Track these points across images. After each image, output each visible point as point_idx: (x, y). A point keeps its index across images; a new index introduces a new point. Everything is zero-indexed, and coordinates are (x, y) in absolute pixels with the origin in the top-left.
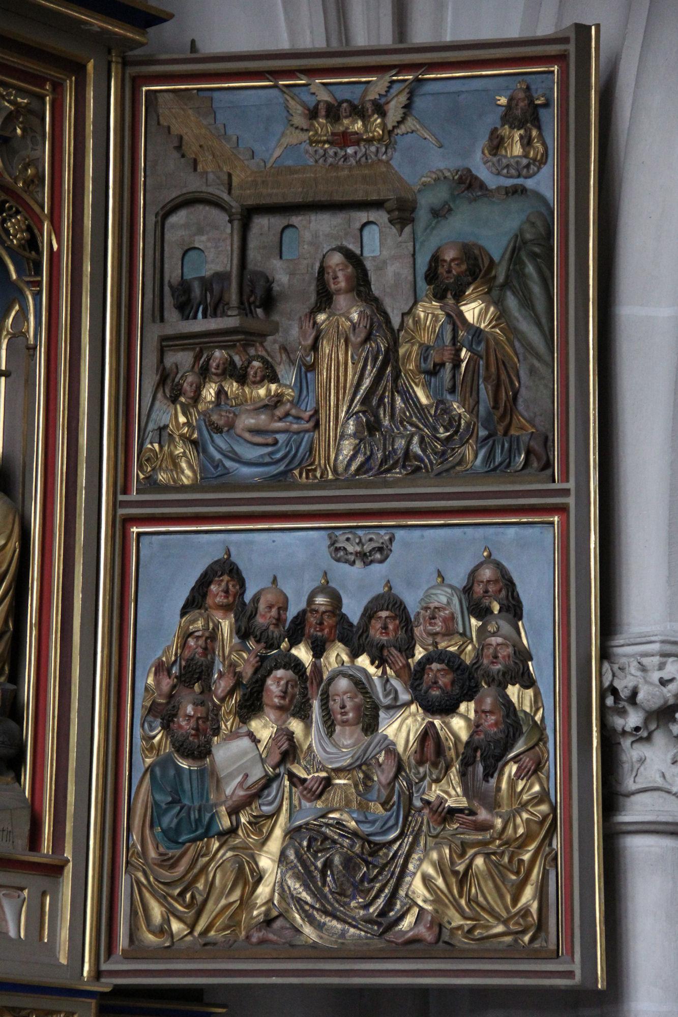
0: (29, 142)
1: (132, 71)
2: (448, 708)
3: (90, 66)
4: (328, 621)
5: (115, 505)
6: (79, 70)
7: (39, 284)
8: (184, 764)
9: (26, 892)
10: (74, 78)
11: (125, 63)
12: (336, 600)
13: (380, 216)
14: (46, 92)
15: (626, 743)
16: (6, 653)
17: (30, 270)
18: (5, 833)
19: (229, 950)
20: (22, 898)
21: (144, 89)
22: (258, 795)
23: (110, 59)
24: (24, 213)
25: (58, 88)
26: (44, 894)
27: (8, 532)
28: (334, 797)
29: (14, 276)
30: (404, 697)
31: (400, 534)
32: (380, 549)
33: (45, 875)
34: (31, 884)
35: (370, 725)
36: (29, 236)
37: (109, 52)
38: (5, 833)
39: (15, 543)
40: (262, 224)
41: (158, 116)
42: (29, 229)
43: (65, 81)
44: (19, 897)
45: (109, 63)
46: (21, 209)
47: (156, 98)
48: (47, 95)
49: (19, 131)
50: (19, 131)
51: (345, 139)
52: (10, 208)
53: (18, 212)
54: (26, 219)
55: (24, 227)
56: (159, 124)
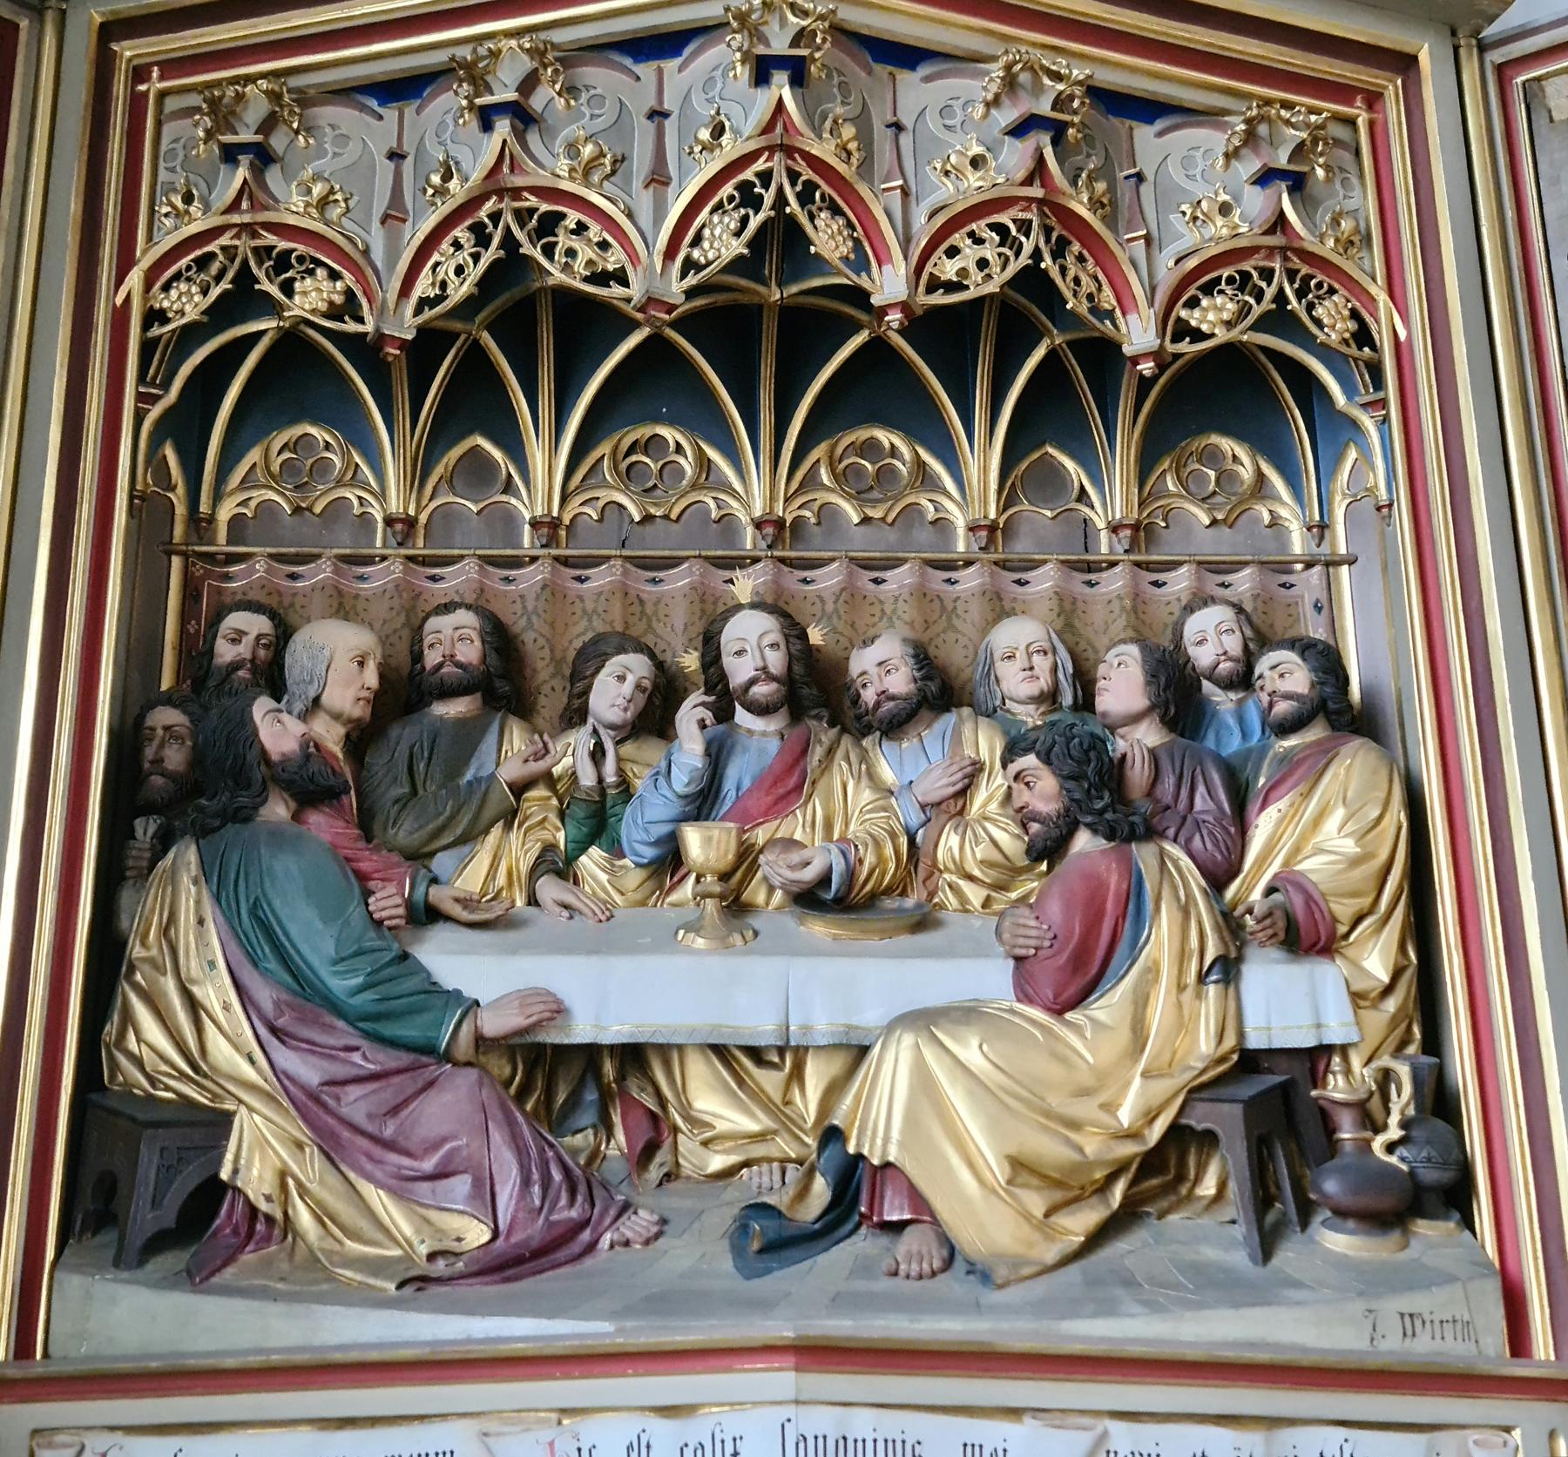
0: (1338, 186)
1: (1497, 56)
3: (1424, 58)
6: (1405, 64)
7: (1383, 403)
9: (1517, 1434)
10: (1399, 82)
11: (1483, 48)
14: (1356, 111)
16: (1411, 1005)
17: (1365, 386)
18: (1459, 1326)
20: (1511, 1444)
21: (1520, 80)
23: (1456, 42)
24: (1342, 291)
25: (1373, 99)
26: (1552, 1435)
27: (1383, 795)
29: (1340, 398)
33: (1547, 1400)
36: (1356, 326)
37: (1454, 33)
38: (1459, 1326)
39: (1398, 815)
41: (1550, 111)
42: (1355, 315)
43: (1386, 87)
44: (1505, 1444)
46: (1336, 286)
47: (1542, 90)
48: (1358, 116)
49: (1320, 172)
50: (1320, 172)
52: (1319, 285)
53: (1332, 291)
54: (1348, 301)
55: (1346, 313)
56: (1551, 120)
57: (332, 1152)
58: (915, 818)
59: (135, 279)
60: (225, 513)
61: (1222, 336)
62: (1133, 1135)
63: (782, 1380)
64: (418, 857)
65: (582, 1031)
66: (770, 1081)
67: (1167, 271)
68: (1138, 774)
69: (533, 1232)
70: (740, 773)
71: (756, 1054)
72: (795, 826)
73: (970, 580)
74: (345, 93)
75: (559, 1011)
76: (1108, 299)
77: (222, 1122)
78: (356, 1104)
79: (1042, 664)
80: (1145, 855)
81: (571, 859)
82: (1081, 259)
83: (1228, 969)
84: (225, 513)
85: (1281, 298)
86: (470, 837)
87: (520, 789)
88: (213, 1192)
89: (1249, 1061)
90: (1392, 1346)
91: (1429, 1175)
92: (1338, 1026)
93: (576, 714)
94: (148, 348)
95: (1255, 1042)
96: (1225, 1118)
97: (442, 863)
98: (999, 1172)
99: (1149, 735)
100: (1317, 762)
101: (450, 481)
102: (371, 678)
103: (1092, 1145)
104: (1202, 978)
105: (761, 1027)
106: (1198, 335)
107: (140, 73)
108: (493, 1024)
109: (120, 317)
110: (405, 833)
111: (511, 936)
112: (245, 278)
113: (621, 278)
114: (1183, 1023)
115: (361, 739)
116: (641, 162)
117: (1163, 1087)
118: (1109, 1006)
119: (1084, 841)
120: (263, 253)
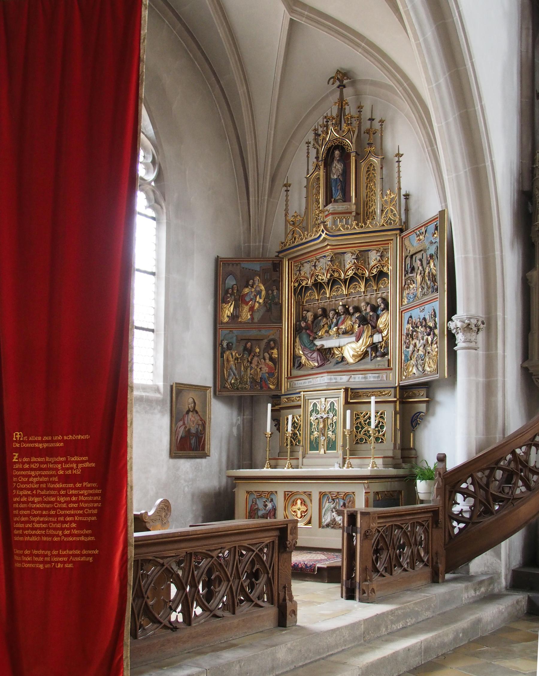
2: (429, 335)
4: (419, 323)
5: (400, 309)
8: (408, 350)
12: (420, 319)
13: (423, 252)
15: (456, 335)
19: (409, 379)
22: (413, 353)
28: (420, 351)
30: (425, 334)
31: (426, 306)
32: (423, 309)
34: (388, 372)
35: (423, 340)
40: (414, 257)
45: (397, 237)
51: (419, 240)
57: (308, 360)
58: (352, 324)
59: (292, 283)
60: (305, 300)
61: (375, 273)
62: (362, 351)
63: (326, 374)
64: (316, 333)
65: (325, 347)
66: (340, 349)
67: (370, 268)
68: (369, 318)
69: (321, 364)
70: (340, 321)
71: (339, 347)
72: (343, 327)
73: (362, 298)
74: (306, 262)
75: (323, 346)
76: (364, 272)
77: (301, 357)
78: (309, 355)
79: (364, 307)
80: (365, 327)
81: (329, 331)
82: (361, 270)
83: (372, 336)
84: (305, 300)
85: (380, 268)
86: (320, 330)
87: (323, 326)
88: (301, 363)
89: (374, 344)
90: (377, 367)
91: (386, 352)
92: (381, 340)
93: (330, 317)
94: (294, 290)
95: (374, 342)
96: (369, 350)
97: (318, 333)
98: (351, 356)
99: (371, 314)
100: (384, 313)
101: (322, 295)
102: (312, 317)
103: (359, 353)
104: (369, 337)
105: (337, 345)
106: (373, 273)
107: (292, 263)
108: (318, 347)
109: (291, 287)
110: (315, 331)
111: (321, 339)
112: (300, 282)
113: (323, 280)
114: (366, 343)
115: (313, 322)
116: (324, 268)
117: (364, 347)
118: (361, 341)
119: (361, 326)
120: (301, 279)
